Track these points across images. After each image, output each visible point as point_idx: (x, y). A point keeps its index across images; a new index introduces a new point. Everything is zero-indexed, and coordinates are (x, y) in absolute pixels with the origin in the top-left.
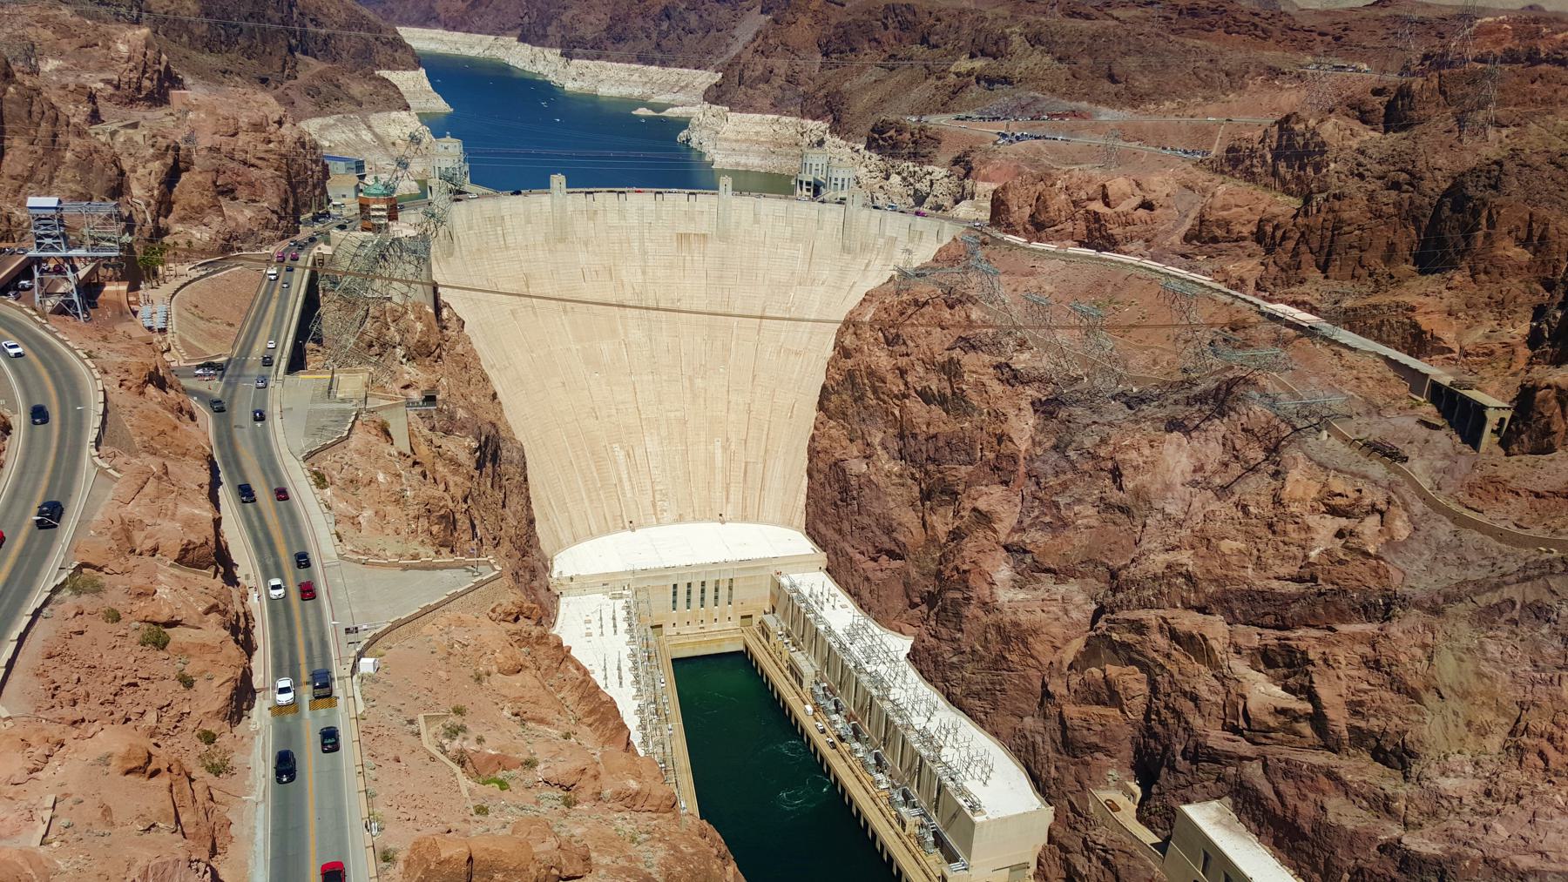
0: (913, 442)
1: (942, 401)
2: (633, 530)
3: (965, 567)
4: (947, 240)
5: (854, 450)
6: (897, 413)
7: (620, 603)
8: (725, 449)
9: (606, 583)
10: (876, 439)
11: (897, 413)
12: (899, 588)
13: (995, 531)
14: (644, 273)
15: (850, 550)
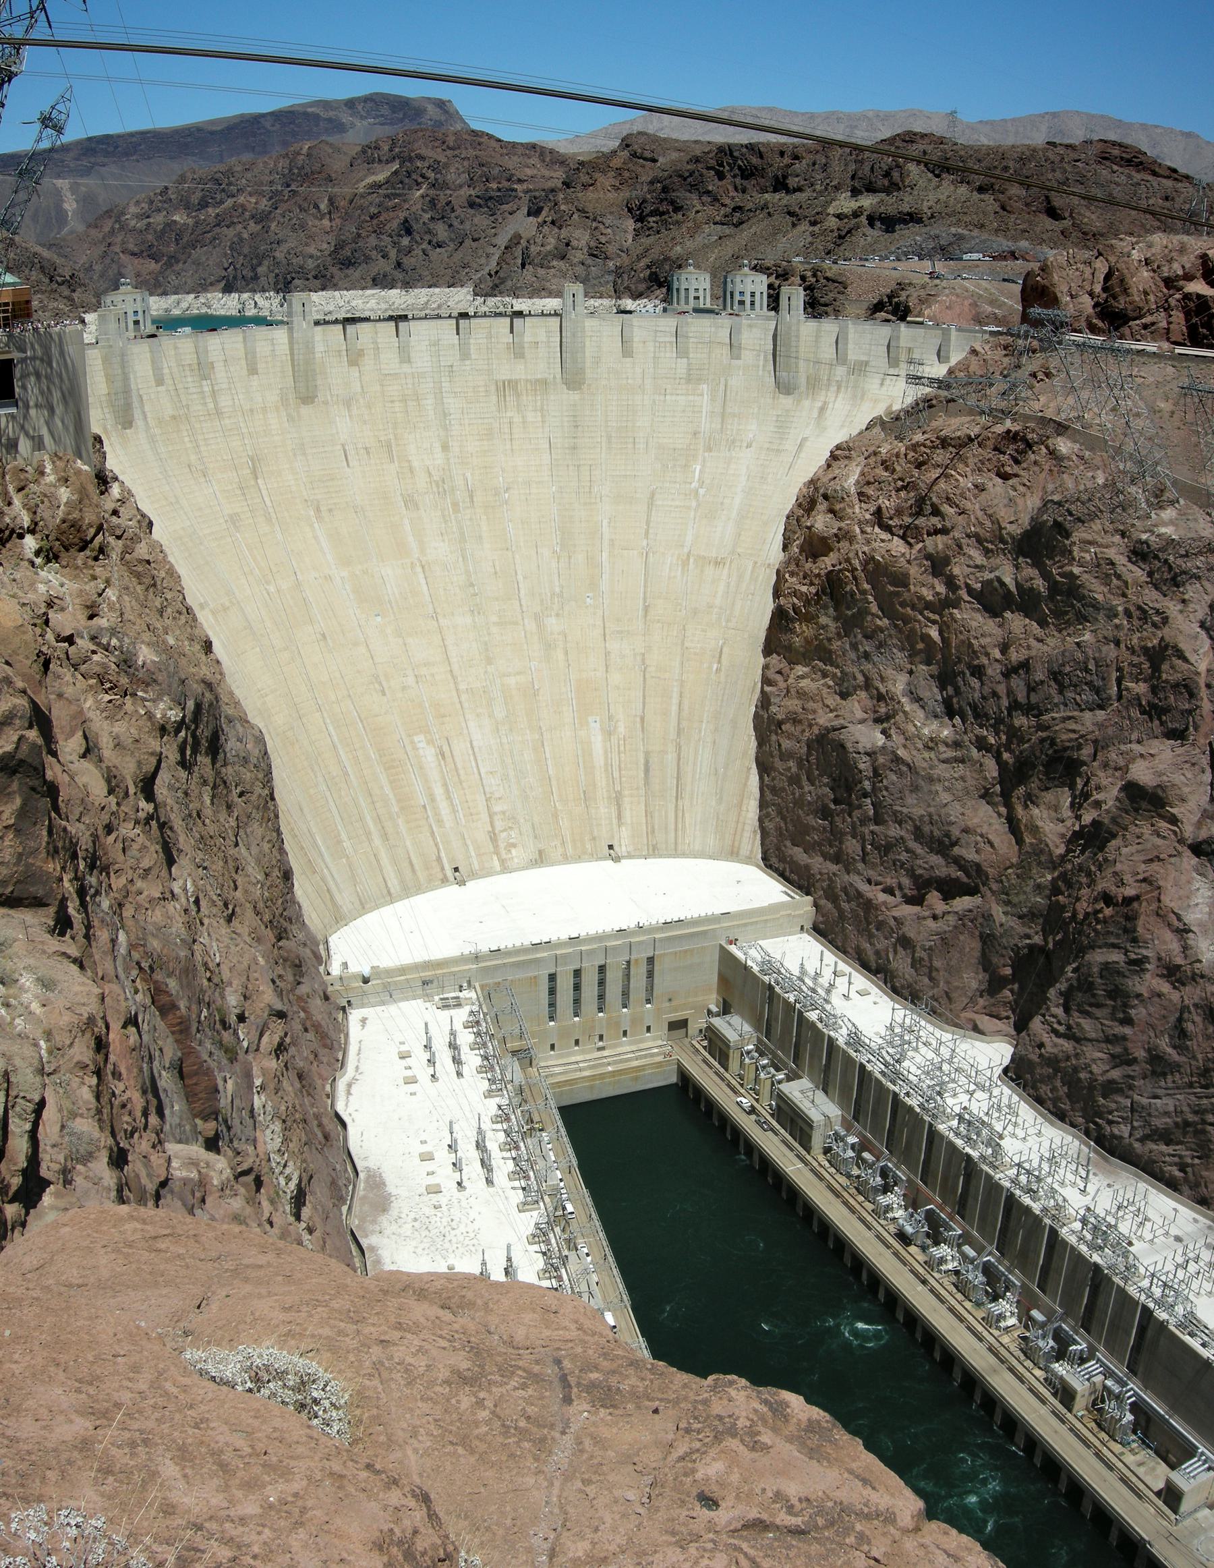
0: (975, 682)
1: (1026, 602)
2: (462, 883)
3: (1130, 892)
4: (956, 358)
5: (856, 706)
6: (934, 633)
7: (461, 1015)
8: (608, 733)
9: (428, 980)
10: (898, 685)
11: (934, 633)
12: (971, 946)
13: (1174, 820)
14: (445, 448)
15: (864, 887)
